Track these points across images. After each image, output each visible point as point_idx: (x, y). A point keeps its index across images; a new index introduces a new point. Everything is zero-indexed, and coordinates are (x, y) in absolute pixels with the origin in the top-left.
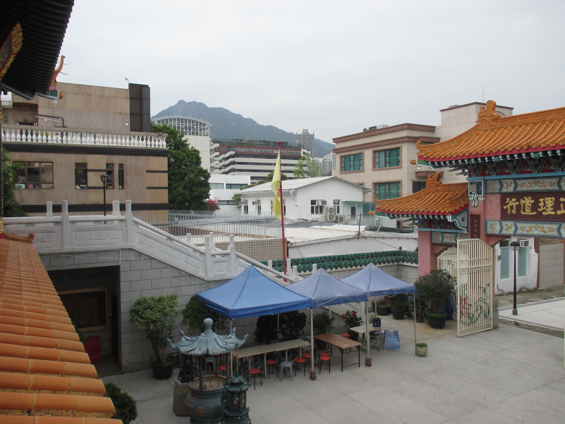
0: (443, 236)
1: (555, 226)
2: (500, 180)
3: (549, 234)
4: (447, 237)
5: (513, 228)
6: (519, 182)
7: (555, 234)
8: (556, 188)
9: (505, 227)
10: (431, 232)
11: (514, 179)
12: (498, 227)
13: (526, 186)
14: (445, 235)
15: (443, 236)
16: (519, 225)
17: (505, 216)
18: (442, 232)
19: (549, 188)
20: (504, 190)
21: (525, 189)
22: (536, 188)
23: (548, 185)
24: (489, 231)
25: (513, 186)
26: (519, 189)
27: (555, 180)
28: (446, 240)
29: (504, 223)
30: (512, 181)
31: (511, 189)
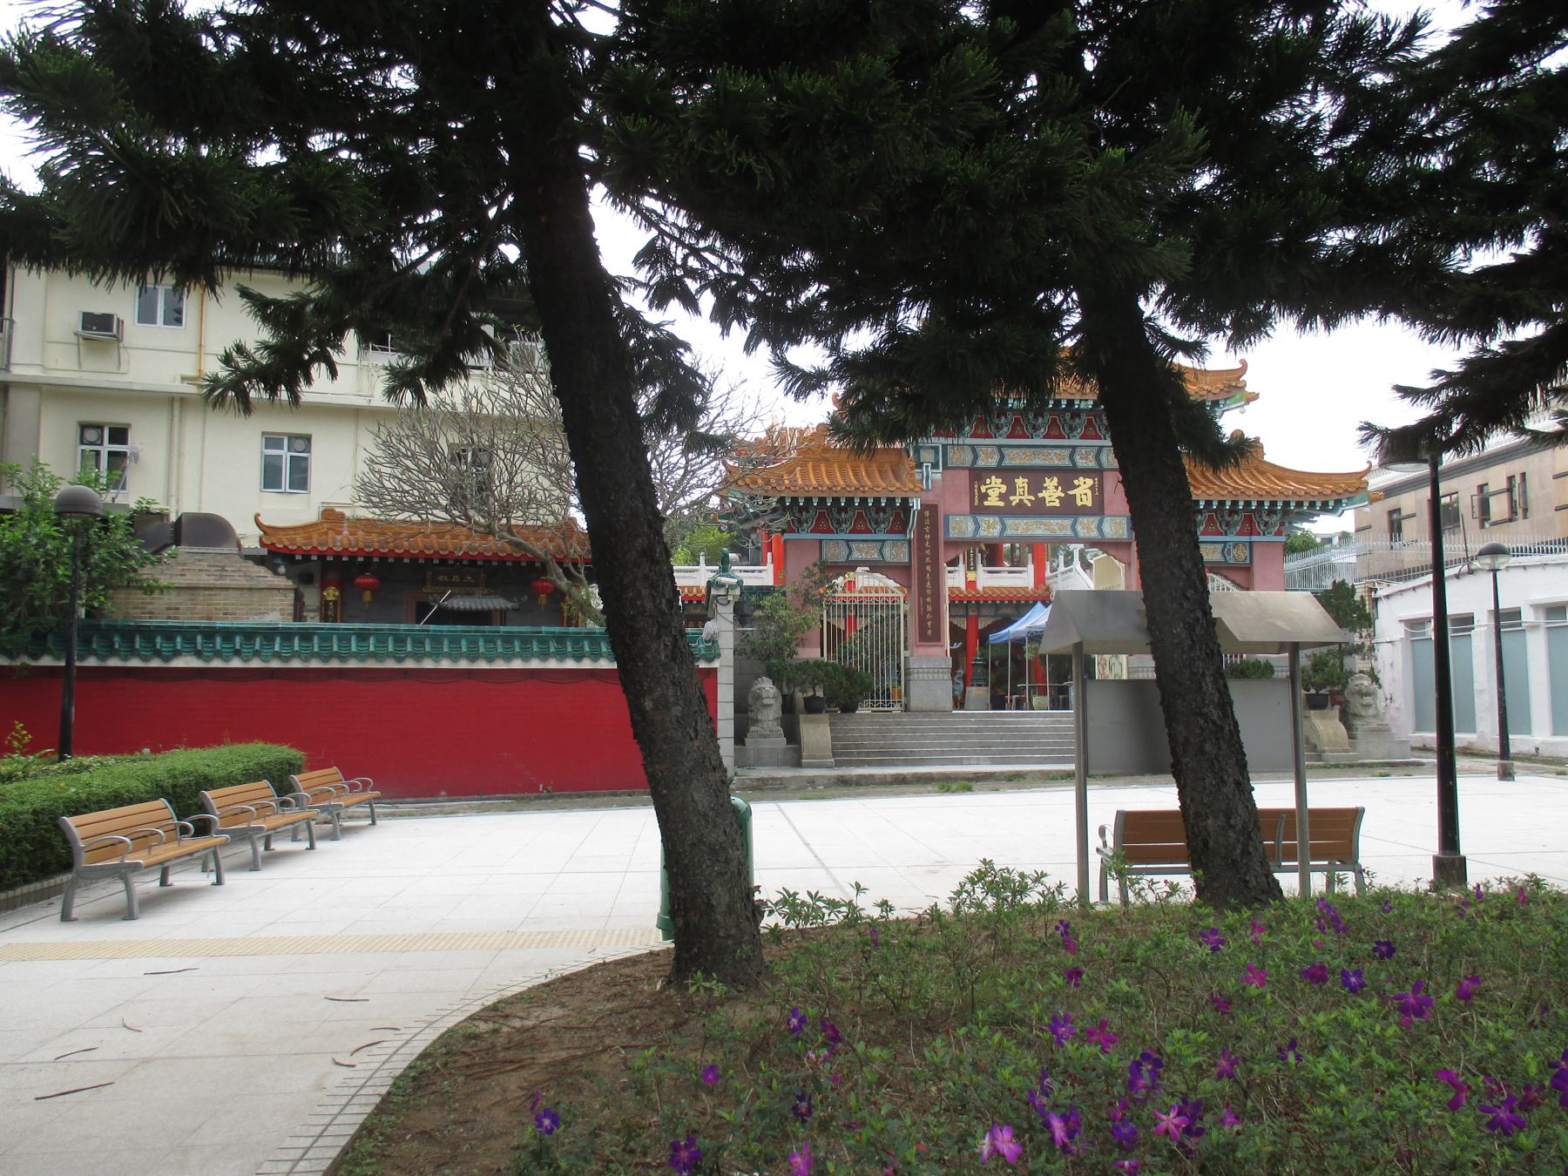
0: (849, 548)
1: (1068, 522)
2: (972, 447)
3: (1059, 533)
4: (859, 550)
5: (999, 527)
6: (1006, 451)
7: (1069, 533)
8: (1067, 463)
9: (983, 526)
10: (821, 541)
11: (1000, 447)
12: (971, 527)
13: (1014, 458)
14: (854, 546)
15: (849, 548)
16: (1009, 522)
17: (978, 509)
18: (847, 541)
19: (1056, 463)
20: (981, 463)
21: (1017, 462)
22: (1038, 461)
23: (1058, 459)
24: (953, 534)
25: (996, 457)
26: (1006, 462)
27: (1067, 452)
28: (856, 555)
29: (981, 519)
30: (995, 449)
31: (993, 462)
